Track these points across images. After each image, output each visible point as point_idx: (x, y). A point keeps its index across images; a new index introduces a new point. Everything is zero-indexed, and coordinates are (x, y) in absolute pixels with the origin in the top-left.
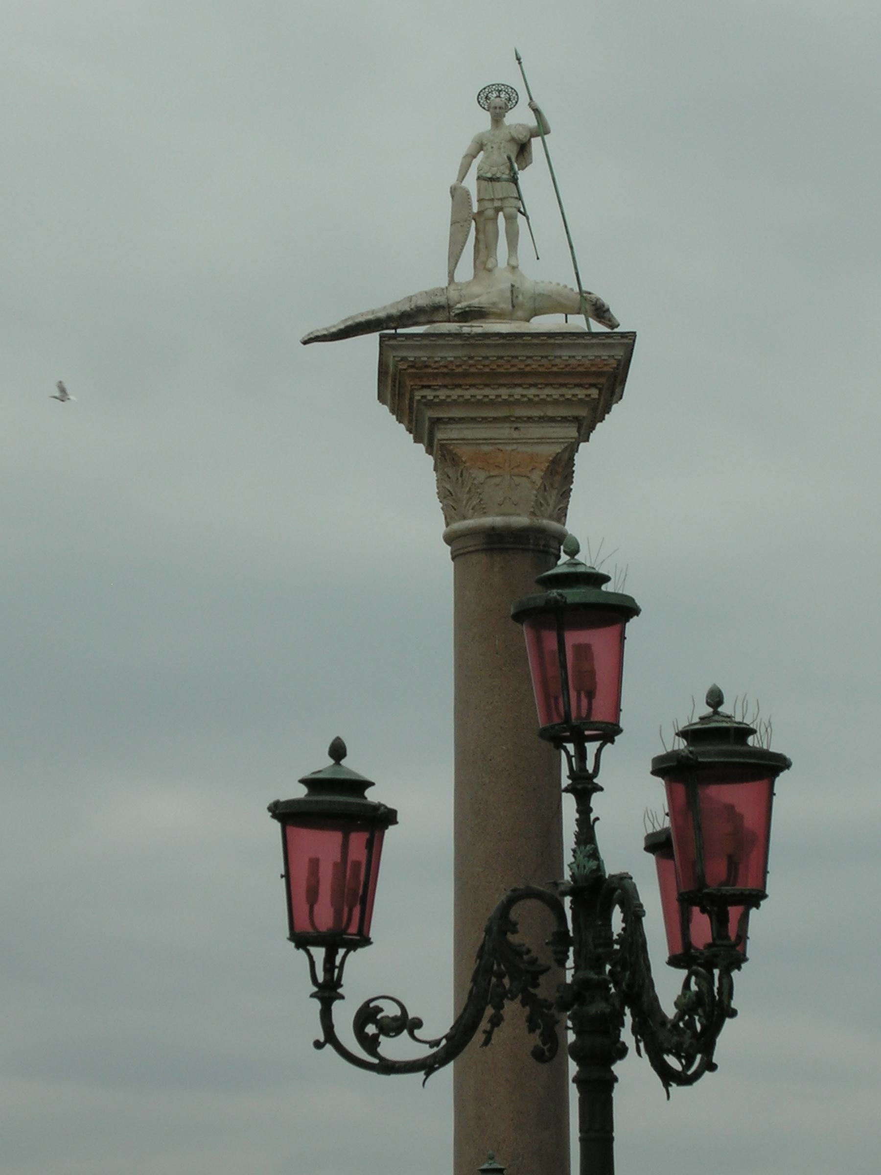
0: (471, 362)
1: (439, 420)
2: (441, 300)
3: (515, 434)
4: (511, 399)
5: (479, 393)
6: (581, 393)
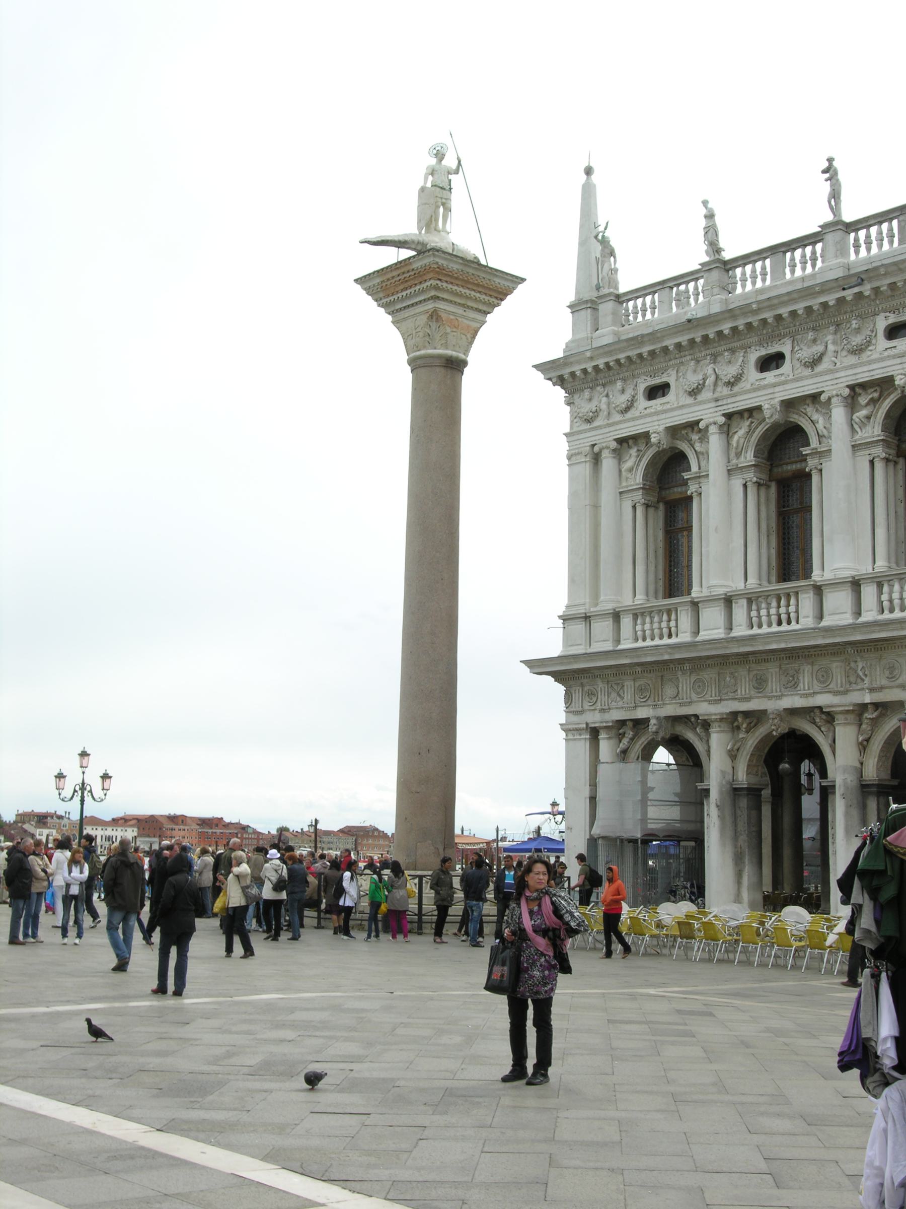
2: (415, 238)
3: (464, 314)
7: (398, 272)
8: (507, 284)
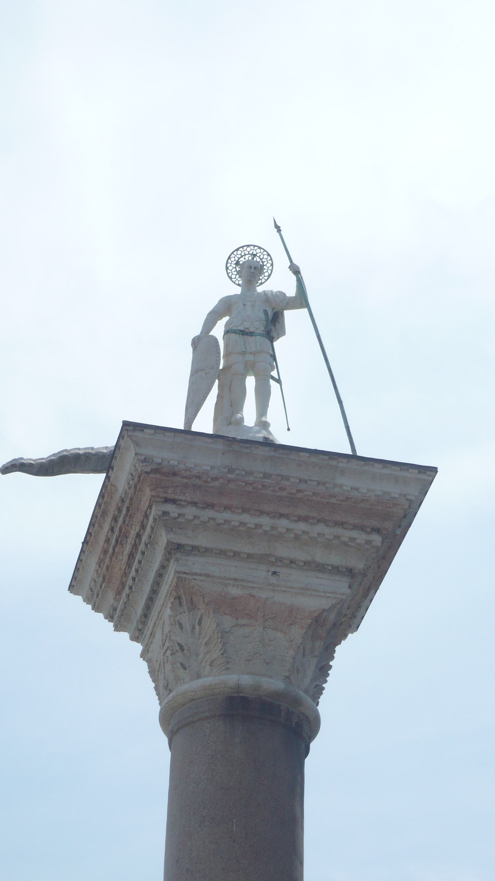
0: (230, 476)
1: (179, 547)
4: (274, 532)
5: (235, 518)
6: (361, 537)
7: (109, 519)
8: (394, 490)
